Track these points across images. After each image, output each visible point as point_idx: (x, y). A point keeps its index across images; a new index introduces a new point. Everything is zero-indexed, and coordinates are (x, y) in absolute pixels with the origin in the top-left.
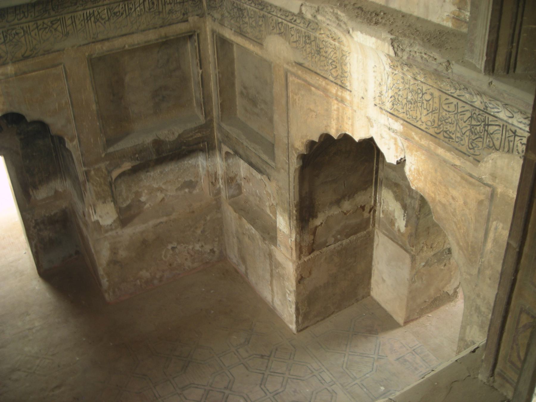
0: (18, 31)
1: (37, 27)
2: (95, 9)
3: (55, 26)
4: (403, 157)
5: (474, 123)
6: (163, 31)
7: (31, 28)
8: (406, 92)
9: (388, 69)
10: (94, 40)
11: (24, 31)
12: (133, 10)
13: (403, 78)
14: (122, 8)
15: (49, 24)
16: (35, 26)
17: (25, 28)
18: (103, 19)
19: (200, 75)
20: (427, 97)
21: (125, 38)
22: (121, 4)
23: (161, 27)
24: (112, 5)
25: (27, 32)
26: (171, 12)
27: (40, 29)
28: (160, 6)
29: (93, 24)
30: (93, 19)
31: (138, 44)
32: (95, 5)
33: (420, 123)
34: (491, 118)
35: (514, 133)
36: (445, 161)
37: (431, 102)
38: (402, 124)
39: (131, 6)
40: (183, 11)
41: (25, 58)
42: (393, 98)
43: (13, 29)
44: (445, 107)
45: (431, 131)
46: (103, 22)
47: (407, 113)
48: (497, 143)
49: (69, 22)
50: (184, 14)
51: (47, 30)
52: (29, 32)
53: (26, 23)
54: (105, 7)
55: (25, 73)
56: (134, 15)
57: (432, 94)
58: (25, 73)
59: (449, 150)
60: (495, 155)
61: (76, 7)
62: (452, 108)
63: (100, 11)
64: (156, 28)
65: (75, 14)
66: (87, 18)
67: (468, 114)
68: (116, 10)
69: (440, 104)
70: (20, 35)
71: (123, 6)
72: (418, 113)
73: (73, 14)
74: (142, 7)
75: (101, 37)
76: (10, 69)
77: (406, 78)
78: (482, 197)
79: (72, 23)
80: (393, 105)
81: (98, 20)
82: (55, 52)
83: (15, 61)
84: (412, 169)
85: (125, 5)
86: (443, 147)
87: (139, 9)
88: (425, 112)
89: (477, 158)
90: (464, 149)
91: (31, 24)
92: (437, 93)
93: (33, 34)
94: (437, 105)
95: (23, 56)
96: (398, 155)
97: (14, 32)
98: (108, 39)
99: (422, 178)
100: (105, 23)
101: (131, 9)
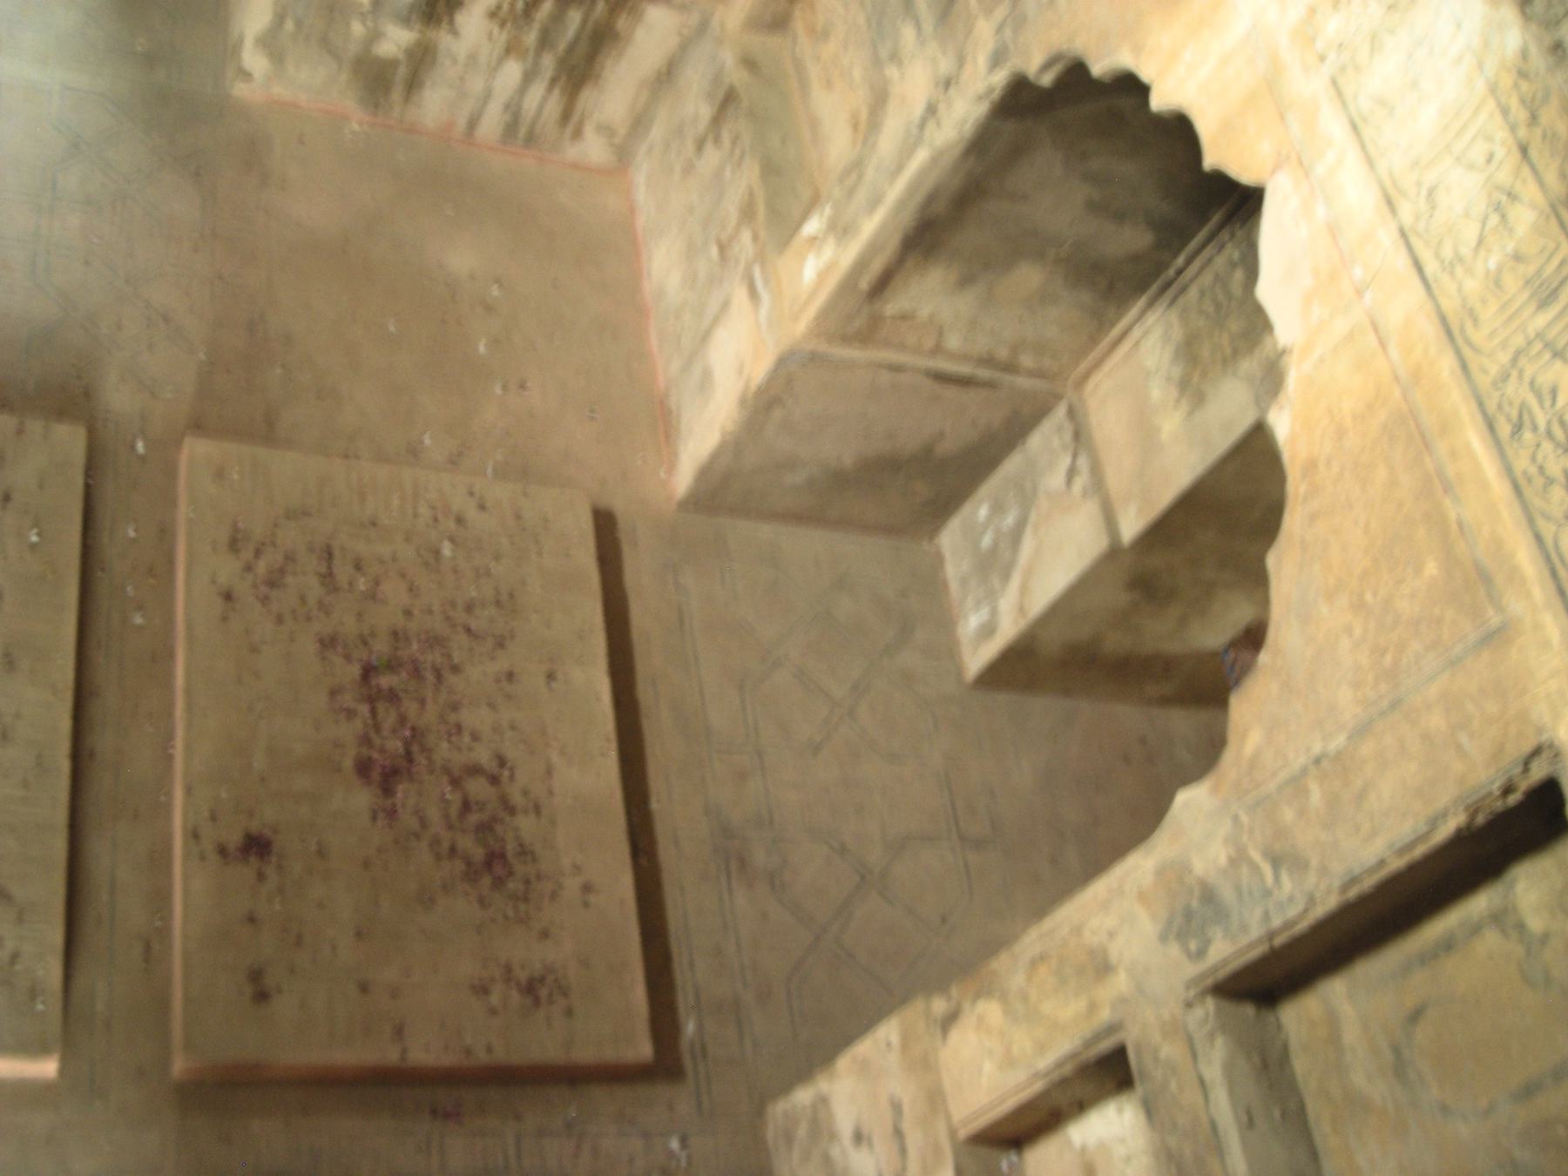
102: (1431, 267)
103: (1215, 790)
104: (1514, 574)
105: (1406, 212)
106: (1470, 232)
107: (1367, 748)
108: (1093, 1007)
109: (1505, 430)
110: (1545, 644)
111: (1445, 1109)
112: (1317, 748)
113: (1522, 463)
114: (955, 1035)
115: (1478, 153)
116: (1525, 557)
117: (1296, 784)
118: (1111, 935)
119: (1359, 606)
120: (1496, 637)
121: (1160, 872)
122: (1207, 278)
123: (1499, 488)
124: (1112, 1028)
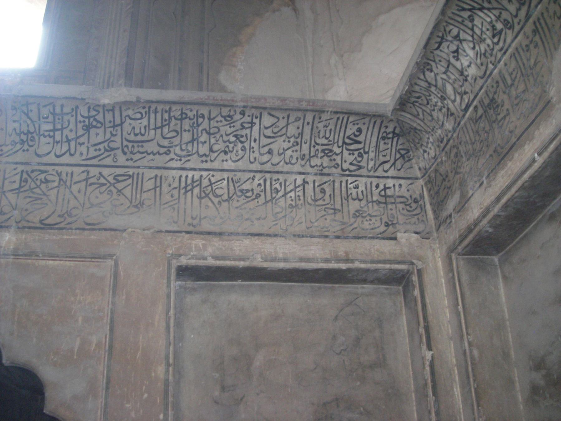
0: (49, 178)
1: (86, 180)
2: (205, 174)
3: (120, 186)
6: (342, 247)
7: (76, 179)
10: (191, 229)
11: (61, 180)
12: (280, 194)
14: (259, 185)
15: (111, 179)
16: (84, 176)
17: (64, 175)
18: (217, 196)
19: (428, 363)
21: (257, 241)
22: (258, 176)
23: (338, 237)
24: (239, 174)
25: (65, 183)
26: (358, 214)
27: (91, 184)
28: (338, 199)
29: (196, 201)
30: (196, 191)
31: (285, 260)
32: (205, 166)
39: (277, 186)
40: (385, 219)
41: (44, 226)
43: (43, 172)
46: (216, 200)
49: (149, 185)
50: (387, 225)
51: (104, 188)
52: (68, 183)
53: (67, 165)
54: (225, 175)
55: (32, 254)
56: (282, 203)
58: (32, 254)
61: (168, 158)
63: (213, 180)
64: (326, 237)
65: (165, 173)
66: (187, 185)
68: (246, 186)
70: (51, 185)
71: (262, 182)
73: (159, 172)
74: (301, 193)
75: (206, 226)
76: (9, 238)
79: (155, 187)
81: (207, 195)
82: (105, 230)
83: (24, 227)
85: (265, 181)
87: (292, 194)
91: (76, 170)
93: (75, 188)
95: (41, 222)
97: (42, 176)
98: (220, 234)
100: (219, 202)
101: (278, 191)
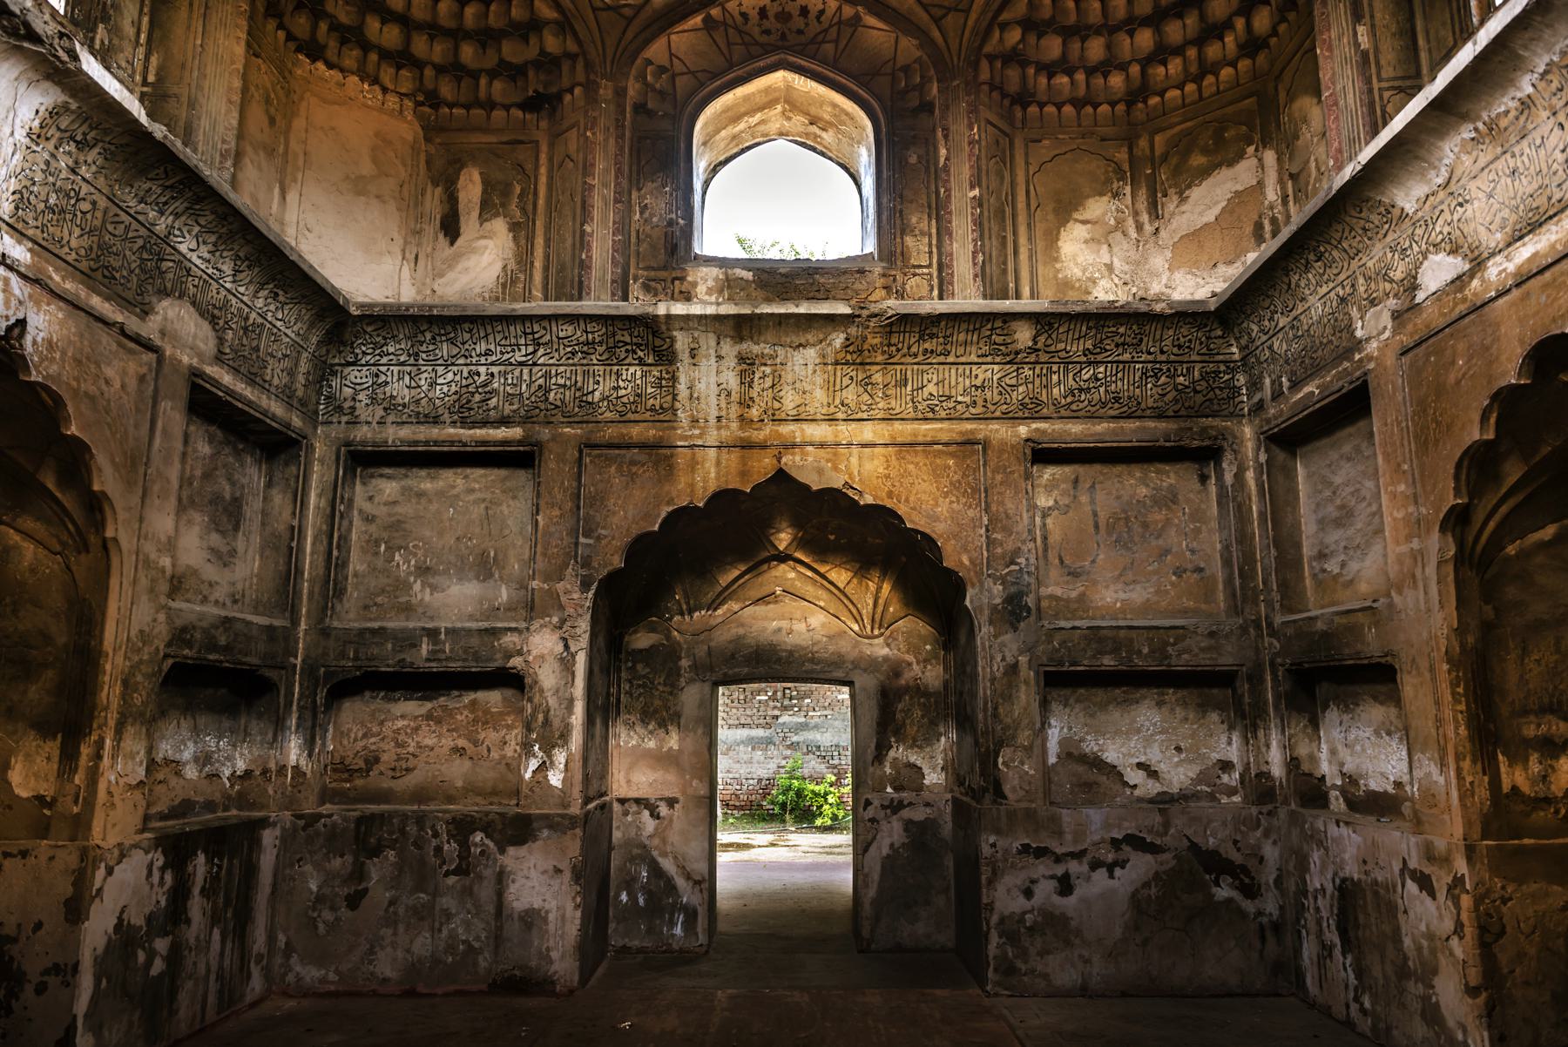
4: (20, 316)
5: (145, 256)
8: (47, 189)
9: (20, 135)
13: (47, 163)
20: (85, 206)
33: (66, 249)
34: (169, 250)
35: (188, 271)
36: (101, 320)
37: (89, 216)
38: (30, 250)
42: (17, 196)
44: (110, 228)
45: (84, 266)
47: (43, 229)
48: (169, 285)
57: (94, 203)
59: (107, 299)
60: (165, 303)
62: (120, 230)
67: (140, 242)
69: (104, 222)
72: (66, 231)
77: (54, 164)
78: (144, 370)
80: (17, 208)
84: (39, 339)
86: (99, 294)
88: (77, 232)
89: (146, 308)
90: (129, 295)
92: (103, 203)
94: (98, 223)
96: (10, 313)
99: (58, 355)
102: (865, 416)
103: (973, 585)
104: (972, 432)
105: (840, 416)
106: (866, 397)
107: (994, 508)
108: (1026, 683)
109: (931, 415)
110: (997, 431)
111: (1093, 561)
112: (983, 531)
113: (943, 414)
114: (1007, 789)
115: (846, 381)
116: (969, 426)
117: (990, 542)
118: (1003, 659)
119: (946, 495)
120: (986, 444)
121: (991, 622)
122: (625, 686)
123: (945, 425)
124: (1037, 673)
